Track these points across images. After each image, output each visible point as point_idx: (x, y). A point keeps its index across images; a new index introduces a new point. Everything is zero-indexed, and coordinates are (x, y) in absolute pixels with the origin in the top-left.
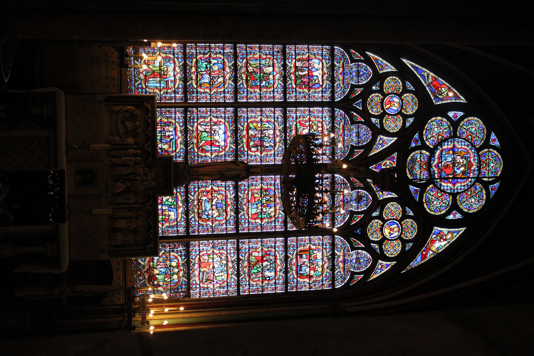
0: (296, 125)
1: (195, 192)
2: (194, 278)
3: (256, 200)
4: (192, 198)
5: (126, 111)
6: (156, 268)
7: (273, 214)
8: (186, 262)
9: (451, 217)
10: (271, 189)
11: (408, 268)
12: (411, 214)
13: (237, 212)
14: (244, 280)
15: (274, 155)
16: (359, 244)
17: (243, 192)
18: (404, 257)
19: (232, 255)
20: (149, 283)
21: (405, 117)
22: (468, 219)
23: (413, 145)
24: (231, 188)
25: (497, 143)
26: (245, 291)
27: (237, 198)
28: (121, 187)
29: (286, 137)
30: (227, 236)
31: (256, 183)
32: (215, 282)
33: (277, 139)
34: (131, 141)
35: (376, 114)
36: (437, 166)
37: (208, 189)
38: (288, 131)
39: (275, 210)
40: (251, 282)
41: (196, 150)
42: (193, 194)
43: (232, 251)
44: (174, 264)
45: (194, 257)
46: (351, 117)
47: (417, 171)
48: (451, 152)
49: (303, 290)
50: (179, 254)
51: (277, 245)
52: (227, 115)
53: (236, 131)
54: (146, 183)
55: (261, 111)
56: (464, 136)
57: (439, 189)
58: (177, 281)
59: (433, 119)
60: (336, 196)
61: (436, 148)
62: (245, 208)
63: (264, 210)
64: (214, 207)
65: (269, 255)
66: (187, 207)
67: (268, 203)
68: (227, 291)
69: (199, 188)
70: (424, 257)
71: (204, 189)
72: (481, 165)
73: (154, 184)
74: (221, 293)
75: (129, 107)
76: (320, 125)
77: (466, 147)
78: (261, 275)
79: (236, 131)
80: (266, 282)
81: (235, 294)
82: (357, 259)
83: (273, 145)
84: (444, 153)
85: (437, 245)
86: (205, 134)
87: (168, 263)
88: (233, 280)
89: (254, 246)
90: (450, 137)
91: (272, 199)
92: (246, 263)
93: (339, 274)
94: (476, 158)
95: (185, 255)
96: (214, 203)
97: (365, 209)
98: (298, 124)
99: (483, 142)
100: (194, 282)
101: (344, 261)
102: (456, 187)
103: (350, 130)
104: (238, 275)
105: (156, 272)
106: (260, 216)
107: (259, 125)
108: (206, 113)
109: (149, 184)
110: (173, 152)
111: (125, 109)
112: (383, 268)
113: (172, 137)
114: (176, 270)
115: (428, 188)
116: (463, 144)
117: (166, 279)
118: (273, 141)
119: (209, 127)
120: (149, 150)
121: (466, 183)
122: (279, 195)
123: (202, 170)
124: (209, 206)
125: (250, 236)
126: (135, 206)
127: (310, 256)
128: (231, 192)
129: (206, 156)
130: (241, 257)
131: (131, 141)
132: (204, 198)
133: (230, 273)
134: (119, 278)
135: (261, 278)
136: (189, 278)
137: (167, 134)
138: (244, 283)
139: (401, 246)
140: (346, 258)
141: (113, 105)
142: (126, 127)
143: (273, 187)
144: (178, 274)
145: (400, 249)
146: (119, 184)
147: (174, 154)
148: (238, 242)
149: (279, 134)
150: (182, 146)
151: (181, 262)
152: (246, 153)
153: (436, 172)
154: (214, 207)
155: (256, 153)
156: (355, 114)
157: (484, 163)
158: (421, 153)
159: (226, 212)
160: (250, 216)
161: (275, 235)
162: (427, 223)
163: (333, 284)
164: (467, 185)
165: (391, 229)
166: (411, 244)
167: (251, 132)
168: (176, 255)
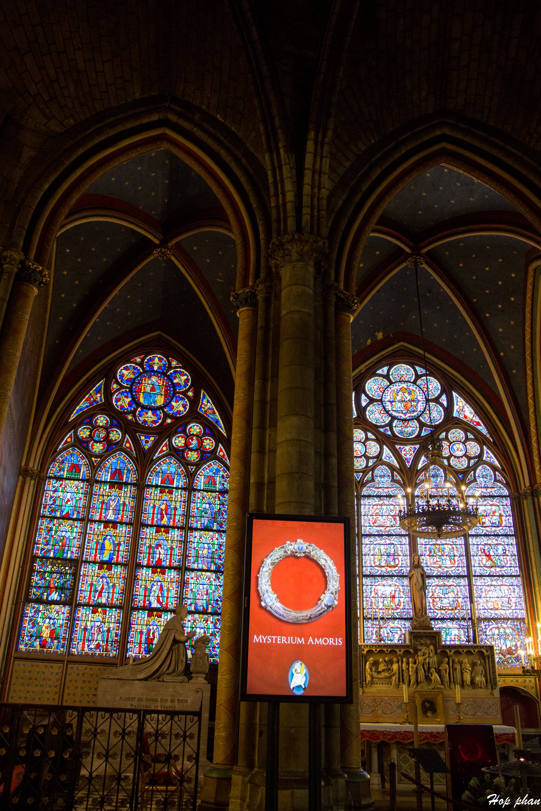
0: (376, 526)
1: (434, 612)
2: (508, 615)
3: (439, 560)
4: (439, 615)
5: (371, 669)
6: (501, 648)
7: (450, 547)
8: (494, 621)
9: (445, 403)
10: (429, 548)
11: (488, 436)
12: (444, 434)
13: (450, 576)
14: (506, 571)
15: (401, 545)
16: (471, 476)
17: (433, 572)
18: (480, 439)
19: (486, 581)
20: (514, 654)
21: (367, 439)
22: (446, 390)
23: (389, 433)
24: (430, 581)
25: (385, 369)
26: (516, 571)
27: (437, 577)
28: (435, 676)
29: (386, 535)
30: (470, 585)
31: (426, 561)
32: (510, 596)
33: (388, 542)
34: (395, 667)
35: (365, 462)
36: (405, 414)
37: (431, 601)
38: (381, 533)
39: (446, 544)
40: (508, 565)
41: (399, 610)
42: (436, 614)
43: (483, 581)
44: (496, 632)
45: (490, 614)
46: (368, 482)
47: (409, 429)
48: (393, 403)
49: (512, 522)
50: (487, 627)
51: (475, 543)
52: (370, 584)
53: (382, 576)
54: (431, 654)
55: (365, 555)
56: (381, 394)
57: (423, 412)
58: (511, 629)
59: (368, 417)
60: (433, 494)
61: (390, 415)
62: (446, 570)
63: (446, 554)
64: (446, 596)
65: (484, 550)
66: (447, 619)
67: (441, 551)
68: (517, 586)
69: (431, 609)
70: (478, 424)
71: (431, 605)
72: (402, 381)
73: (432, 647)
74: (519, 591)
75: (367, 667)
76: (375, 507)
77: (389, 392)
78: (502, 557)
79: (382, 576)
80: (507, 552)
81: (520, 579)
82: (483, 477)
83: (392, 546)
84: (394, 409)
85: (467, 413)
86: (385, 602)
87: (496, 637)
88: (507, 581)
89: (477, 562)
90: (382, 404)
91: (438, 547)
92: (493, 569)
93: (496, 492)
94: (397, 384)
95: (489, 622)
96: (443, 596)
97: (442, 470)
98: (376, 525)
99: (384, 380)
100: (511, 614)
101: (486, 488)
102: (421, 400)
103: (379, 483)
104: (503, 576)
105: (504, 648)
106: (452, 557)
107: (376, 557)
108: (367, 601)
109: (432, 651)
110: (401, 630)
111: (369, 670)
112: (489, 456)
113: (389, 631)
114: (502, 630)
115: (423, 421)
116: (386, 394)
117: (510, 639)
118: (390, 546)
119: (379, 599)
120: (403, 650)
121: (418, 392)
122: (434, 541)
123: (418, 606)
124: (445, 601)
125: (469, 566)
126: (451, 664)
127: (483, 516)
128: (433, 581)
129: (404, 602)
130: (487, 574)
131: (395, 667)
132: (439, 605)
133: (501, 583)
134: (512, 681)
135: (505, 557)
136: (508, 619)
137: (386, 635)
138: (510, 571)
139: (470, 442)
140: (483, 486)
141: (365, 681)
142: (383, 670)
143: (428, 546)
144: (504, 628)
145: (473, 443)
146: (433, 678)
147: (402, 629)
148: (475, 576)
149: (384, 541)
150: (396, 622)
151: (495, 626)
152: (400, 568)
153: (409, 415)
154: (446, 596)
155: (400, 560)
156: (366, 479)
157: (401, 378)
158: (395, 427)
159: (450, 586)
160: (452, 565)
161: (467, 545)
162: (450, 421)
163: (505, 496)
164: (419, 391)
165: (458, 450)
166: (469, 434)
167: (383, 564)
168: (489, 629)
